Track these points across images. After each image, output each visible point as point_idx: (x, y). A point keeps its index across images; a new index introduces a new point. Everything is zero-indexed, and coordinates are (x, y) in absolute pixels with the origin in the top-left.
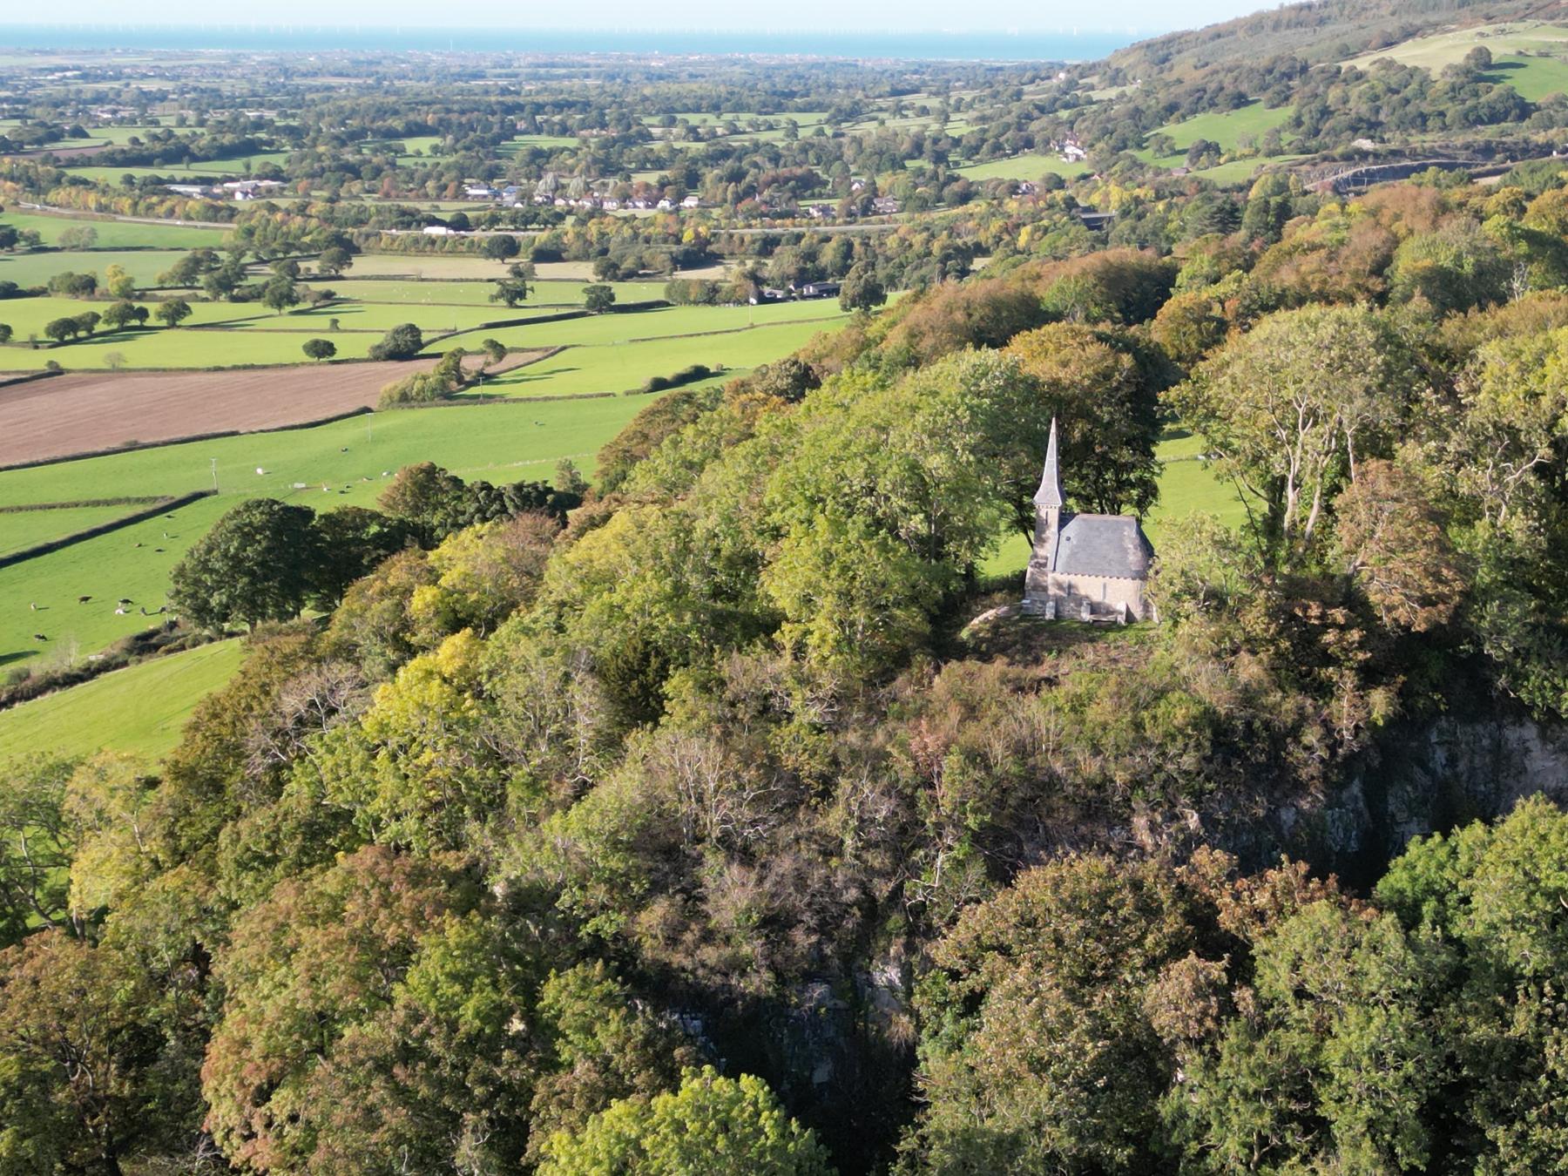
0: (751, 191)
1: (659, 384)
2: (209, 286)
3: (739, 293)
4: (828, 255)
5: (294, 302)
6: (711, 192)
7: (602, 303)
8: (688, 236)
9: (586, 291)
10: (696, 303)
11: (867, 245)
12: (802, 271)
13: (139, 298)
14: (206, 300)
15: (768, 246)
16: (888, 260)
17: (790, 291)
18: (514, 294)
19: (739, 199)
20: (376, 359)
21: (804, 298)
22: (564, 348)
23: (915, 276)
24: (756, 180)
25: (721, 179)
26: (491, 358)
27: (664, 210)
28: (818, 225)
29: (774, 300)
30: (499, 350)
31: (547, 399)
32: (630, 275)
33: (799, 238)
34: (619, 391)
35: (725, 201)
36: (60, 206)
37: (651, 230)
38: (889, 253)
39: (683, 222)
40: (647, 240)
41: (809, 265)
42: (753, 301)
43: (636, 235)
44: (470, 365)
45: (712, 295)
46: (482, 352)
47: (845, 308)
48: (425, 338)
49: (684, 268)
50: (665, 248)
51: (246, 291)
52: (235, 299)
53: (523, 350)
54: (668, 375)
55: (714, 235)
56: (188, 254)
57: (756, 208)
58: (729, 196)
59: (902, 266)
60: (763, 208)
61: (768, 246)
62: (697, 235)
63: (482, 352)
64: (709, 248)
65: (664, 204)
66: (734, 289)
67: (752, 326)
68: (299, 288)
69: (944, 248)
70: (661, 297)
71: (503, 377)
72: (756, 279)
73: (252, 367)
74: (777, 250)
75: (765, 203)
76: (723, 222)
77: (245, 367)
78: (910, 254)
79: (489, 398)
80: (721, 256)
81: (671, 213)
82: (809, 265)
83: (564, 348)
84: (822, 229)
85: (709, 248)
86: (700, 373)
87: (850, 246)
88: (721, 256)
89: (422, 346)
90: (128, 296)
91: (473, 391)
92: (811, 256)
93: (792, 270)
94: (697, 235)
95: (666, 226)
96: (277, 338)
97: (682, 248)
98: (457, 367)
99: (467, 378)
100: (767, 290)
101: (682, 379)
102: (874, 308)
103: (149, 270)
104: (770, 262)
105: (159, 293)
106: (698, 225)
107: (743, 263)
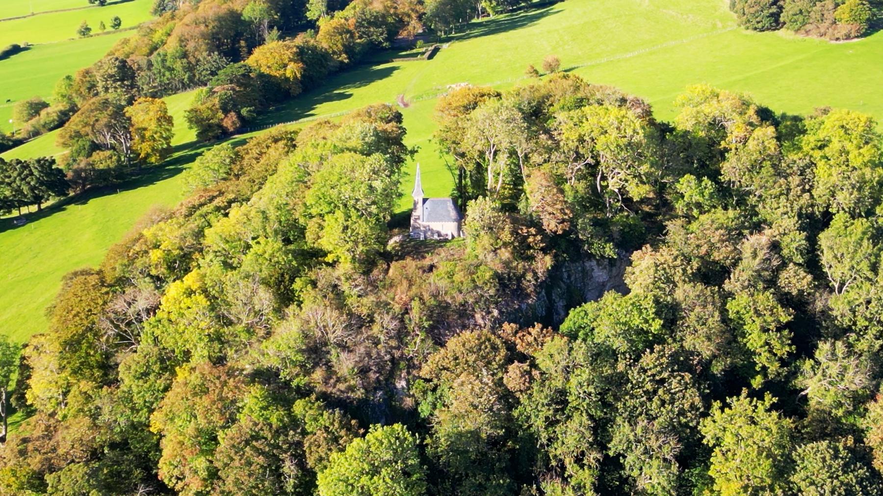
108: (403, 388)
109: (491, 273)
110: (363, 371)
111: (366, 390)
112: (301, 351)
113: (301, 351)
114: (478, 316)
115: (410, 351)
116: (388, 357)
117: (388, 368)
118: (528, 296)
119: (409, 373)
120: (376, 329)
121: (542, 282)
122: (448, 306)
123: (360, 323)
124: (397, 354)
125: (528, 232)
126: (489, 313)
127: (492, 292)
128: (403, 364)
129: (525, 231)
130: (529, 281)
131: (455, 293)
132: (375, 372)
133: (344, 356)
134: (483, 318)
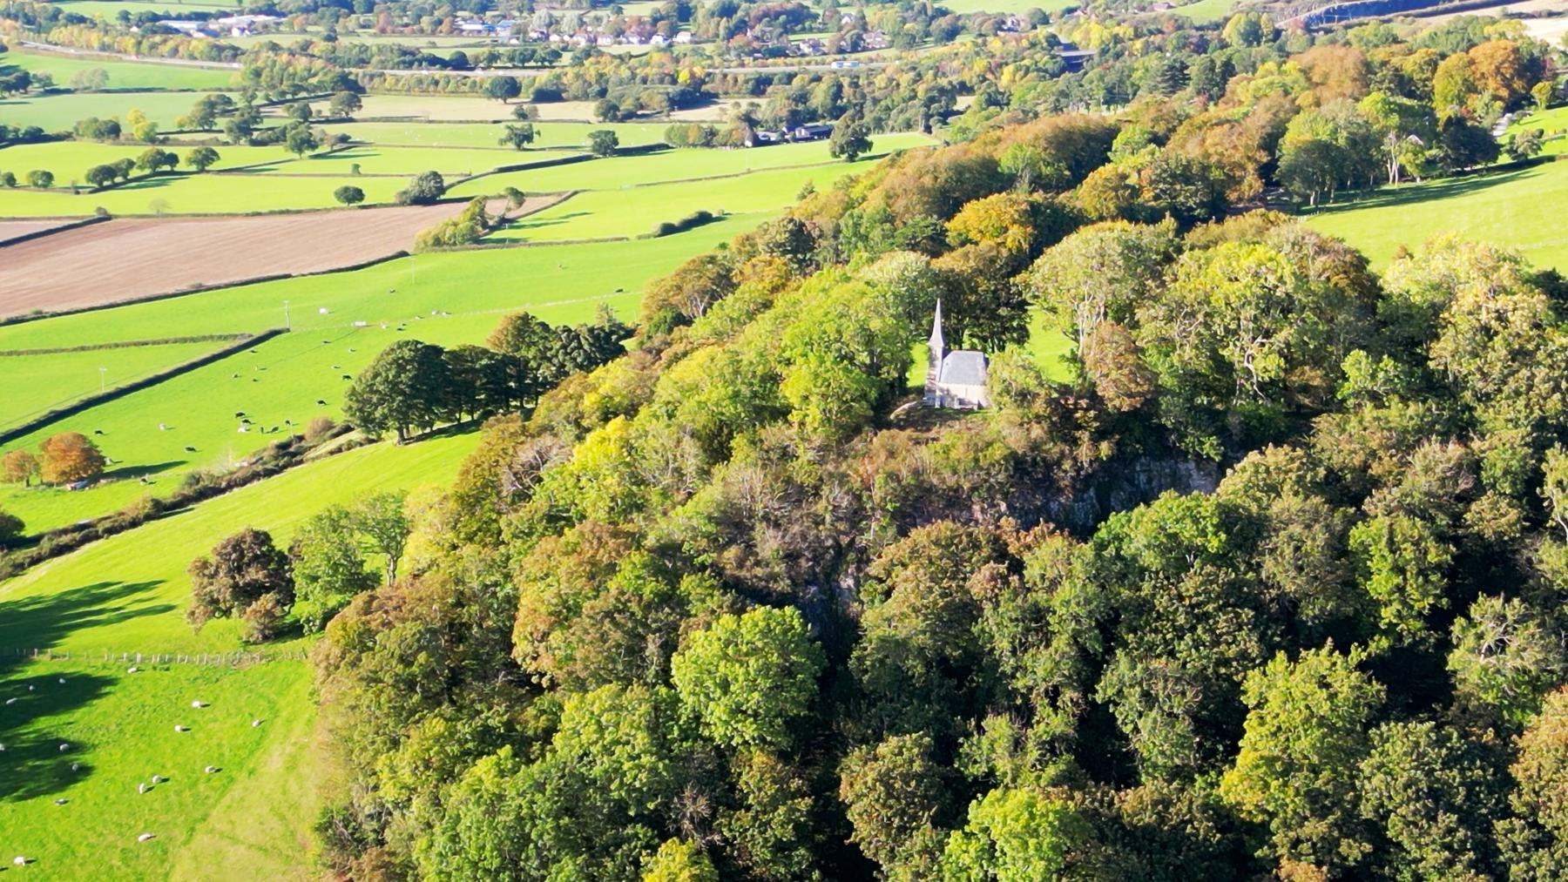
0: (742, 27)
1: (668, 230)
2: (230, 130)
3: (735, 136)
4: (819, 97)
5: (313, 146)
6: (704, 26)
7: (608, 147)
8: (683, 77)
9: (592, 135)
10: (695, 146)
11: (855, 85)
12: (794, 113)
13: (163, 142)
14: (227, 144)
15: (760, 86)
16: (876, 101)
17: (784, 134)
18: (522, 139)
19: (731, 34)
20: (403, 204)
21: (796, 140)
22: (576, 193)
23: (902, 117)
24: (748, 14)
25: (713, 15)
26: (511, 203)
27: (660, 50)
28: (809, 63)
29: (768, 143)
30: (518, 196)
31: (567, 243)
32: (629, 116)
33: (790, 78)
34: (632, 236)
35: (717, 36)
36: (62, 45)
37: (648, 70)
38: (877, 94)
39: (677, 60)
40: (644, 81)
41: (801, 107)
42: (748, 143)
43: (634, 76)
44: (494, 210)
45: (709, 139)
46: (501, 197)
47: (834, 155)
48: (445, 184)
49: (681, 108)
50: (661, 88)
51: (265, 136)
52: (255, 143)
53: (538, 195)
54: (676, 221)
55: (709, 75)
56: (202, 96)
57: (749, 44)
58: (722, 32)
59: (888, 109)
60: (756, 45)
61: (760, 86)
62: (693, 75)
63: (501, 197)
64: (704, 88)
65: (658, 40)
66: (730, 133)
67: (749, 172)
68: (317, 130)
69: (927, 91)
70: (662, 141)
71: (522, 221)
72: (750, 121)
73: (288, 212)
74: (770, 89)
75: (757, 38)
76: (717, 60)
77: (281, 212)
78: (896, 97)
79: (515, 241)
80: (716, 96)
81: (664, 50)
82: (801, 107)
83: (576, 193)
84: (812, 68)
85: (704, 88)
86: (704, 219)
87: (840, 87)
88: (716, 96)
89: (442, 190)
90: (153, 141)
91: (497, 235)
92: (803, 98)
93: (784, 113)
94: (693, 75)
95: (662, 65)
96: (306, 183)
97: (678, 88)
98: (482, 213)
99: (491, 223)
100: (761, 133)
101: (688, 225)
102: (861, 155)
103: (173, 111)
104: (762, 101)
105: (182, 137)
106: (693, 64)
107: (738, 105)
108: (849, 588)
109: (1007, 452)
110: (791, 557)
111: (793, 581)
112: (710, 518)
113: (710, 518)
114: (976, 508)
115: (863, 540)
116: (830, 542)
117: (828, 557)
118: (1060, 491)
119: (859, 569)
120: (820, 507)
121: (1088, 476)
122: (931, 490)
123: (798, 494)
124: (845, 540)
125: (1075, 404)
126: (993, 506)
127: (1001, 477)
128: (852, 556)
129: (1071, 401)
130: (1065, 472)
131: (947, 474)
132: (808, 560)
133: (771, 532)
134: (983, 511)
